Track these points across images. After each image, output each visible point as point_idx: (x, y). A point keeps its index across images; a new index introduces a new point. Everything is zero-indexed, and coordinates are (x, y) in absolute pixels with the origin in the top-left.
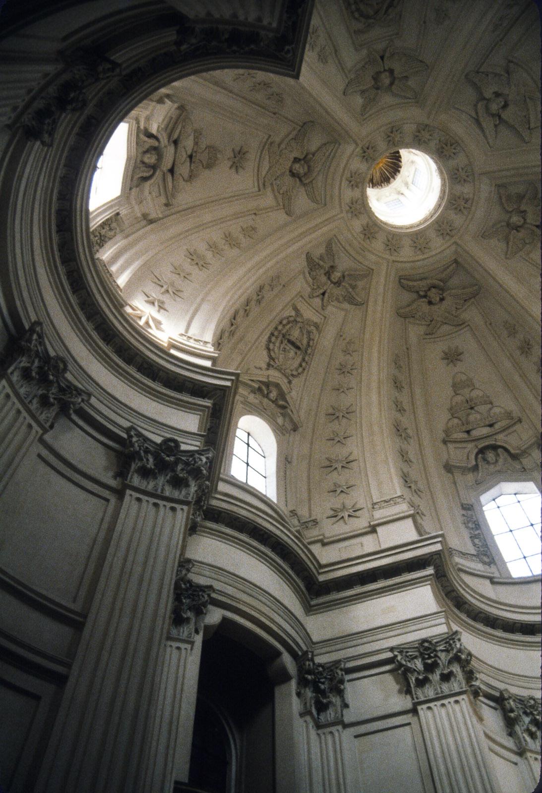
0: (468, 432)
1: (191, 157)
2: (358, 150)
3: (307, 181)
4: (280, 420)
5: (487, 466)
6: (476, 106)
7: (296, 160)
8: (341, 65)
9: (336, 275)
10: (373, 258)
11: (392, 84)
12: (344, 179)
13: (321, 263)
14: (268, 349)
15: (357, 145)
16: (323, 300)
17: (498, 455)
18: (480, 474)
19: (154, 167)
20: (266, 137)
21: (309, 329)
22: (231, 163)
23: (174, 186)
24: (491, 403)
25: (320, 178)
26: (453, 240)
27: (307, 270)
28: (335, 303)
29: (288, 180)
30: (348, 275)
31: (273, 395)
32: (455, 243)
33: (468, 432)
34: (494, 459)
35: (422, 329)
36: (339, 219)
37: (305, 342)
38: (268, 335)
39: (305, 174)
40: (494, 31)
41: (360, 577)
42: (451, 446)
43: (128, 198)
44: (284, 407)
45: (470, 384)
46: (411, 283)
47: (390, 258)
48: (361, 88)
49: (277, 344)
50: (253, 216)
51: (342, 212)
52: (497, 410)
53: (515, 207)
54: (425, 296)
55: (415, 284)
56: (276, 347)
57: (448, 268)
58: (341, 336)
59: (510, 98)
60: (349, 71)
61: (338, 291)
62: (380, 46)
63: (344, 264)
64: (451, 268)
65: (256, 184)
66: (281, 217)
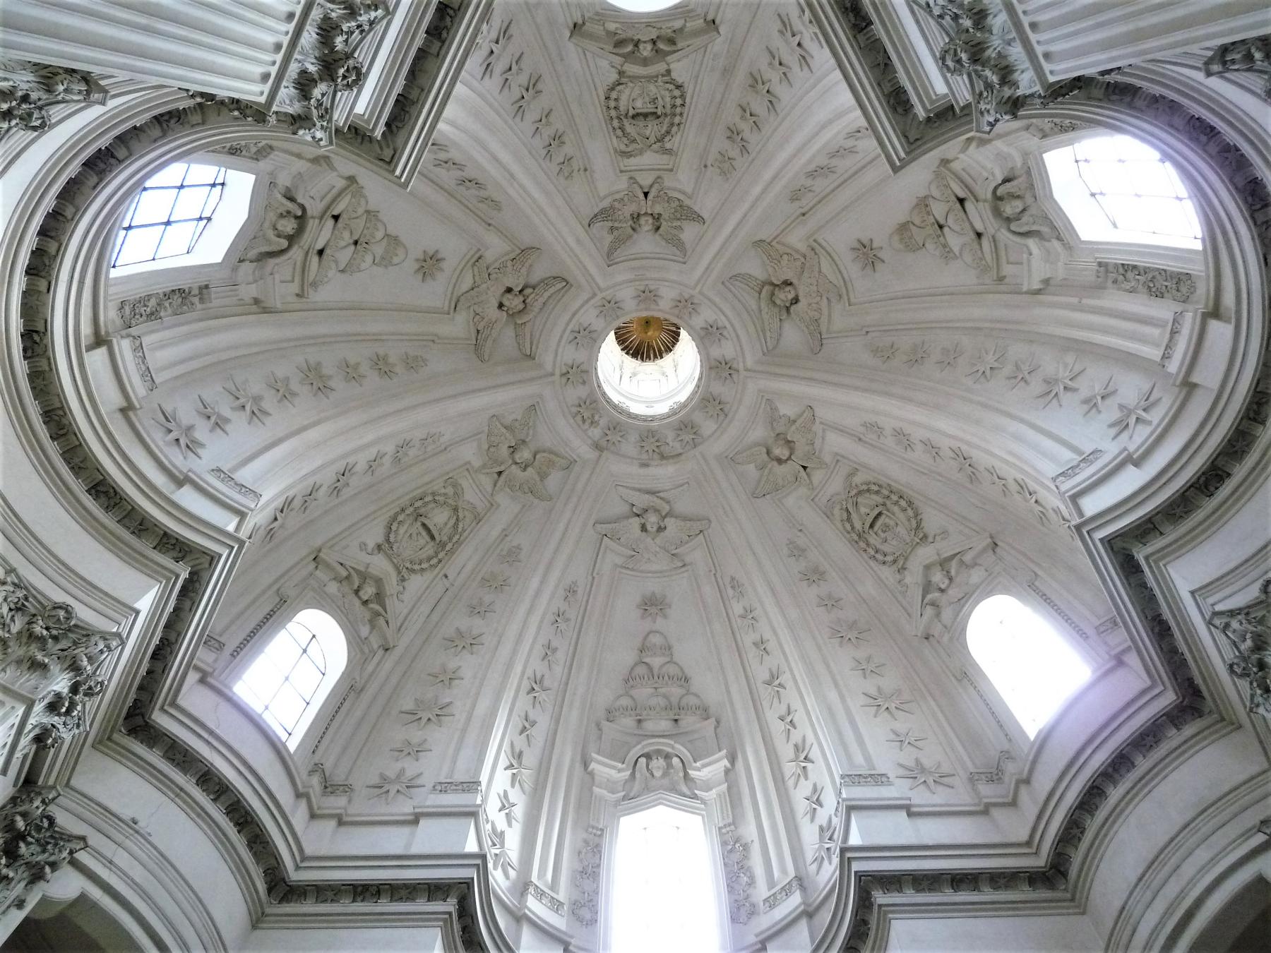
0: (336, 218)
1: (941, 227)
2: (741, 365)
3: (764, 291)
4: (612, 27)
5: (279, 211)
6: (668, 502)
7: (796, 300)
8: (842, 430)
9: (646, 224)
10: (620, 278)
11: (768, 453)
12: (728, 326)
13: (678, 223)
14: (678, 87)
15: (747, 370)
16: (641, 187)
17: (279, 236)
18: (279, 196)
19: (997, 198)
20: (853, 300)
21: (634, 146)
22: (875, 246)
23: (947, 186)
24: (342, 271)
25: (753, 304)
26: (558, 372)
27: (687, 202)
28: (617, 196)
29: (789, 275)
30: (630, 237)
31: (646, 50)
32: (552, 374)
33: (336, 218)
34: (280, 228)
35: (490, 256)
36: (696, 285)
37: (629, 128)
38: (688, 100)
39: (773, 294)
40: (733, 579)
41: (451, 12)
42: (341, 183)
43: (1026, 155)
44: (620, 43)
45: (385, 261)
46: (552, 290)
47: (604, 294)
48: (797, 424)
49: (668, 99)
50: (803, 211)
51: (700, 293)
52: (331, 274)
53: (536, 463)
54: (521, 291)
55: (546, 295)
56: (665, 97)
57: (531, 344)
58: (586, 170)
59: (649, 540)
60: (824, 431)
61: (633, 208)
62: (817, 476)
63: (646, 242)
64: (528, 345)
65: (824, 244)
66: (765, 234)
